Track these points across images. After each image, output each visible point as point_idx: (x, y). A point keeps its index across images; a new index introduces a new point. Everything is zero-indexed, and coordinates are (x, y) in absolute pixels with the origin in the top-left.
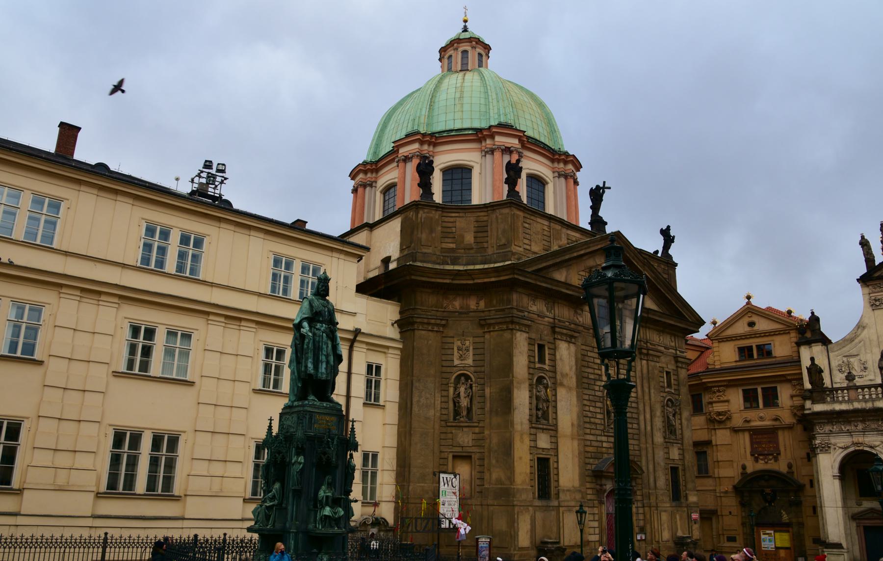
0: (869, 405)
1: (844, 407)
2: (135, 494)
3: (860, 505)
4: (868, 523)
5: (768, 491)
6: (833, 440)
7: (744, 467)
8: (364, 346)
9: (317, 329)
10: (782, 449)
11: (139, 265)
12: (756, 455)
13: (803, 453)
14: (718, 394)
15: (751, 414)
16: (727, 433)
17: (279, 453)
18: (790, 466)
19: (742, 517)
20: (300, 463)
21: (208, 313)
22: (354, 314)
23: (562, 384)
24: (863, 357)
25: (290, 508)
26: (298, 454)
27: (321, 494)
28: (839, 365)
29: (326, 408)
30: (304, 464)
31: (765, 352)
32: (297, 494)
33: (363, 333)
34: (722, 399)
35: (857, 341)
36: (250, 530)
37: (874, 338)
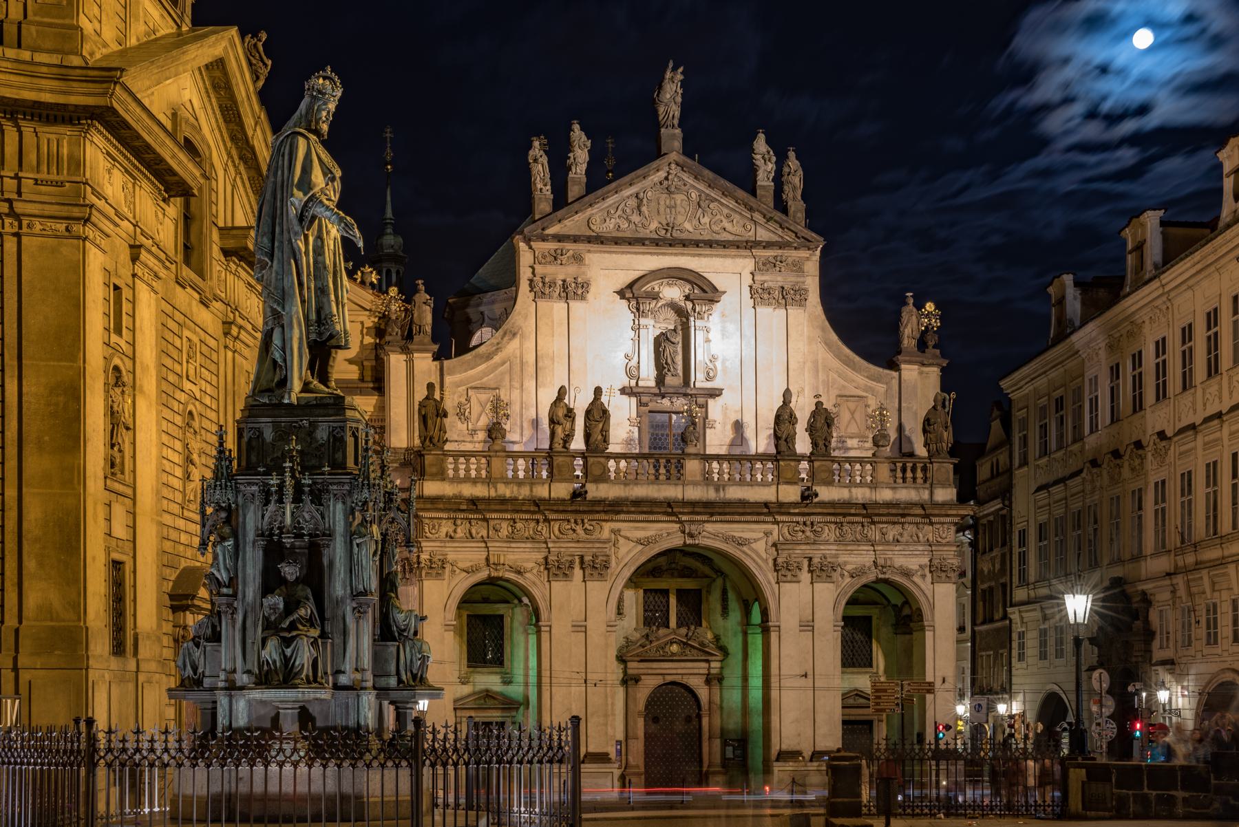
0: (524, 492)
1: (480, 491)
23: (142, 391)
24: (504, 395)
28: (460, 405)
35: (497, 359)
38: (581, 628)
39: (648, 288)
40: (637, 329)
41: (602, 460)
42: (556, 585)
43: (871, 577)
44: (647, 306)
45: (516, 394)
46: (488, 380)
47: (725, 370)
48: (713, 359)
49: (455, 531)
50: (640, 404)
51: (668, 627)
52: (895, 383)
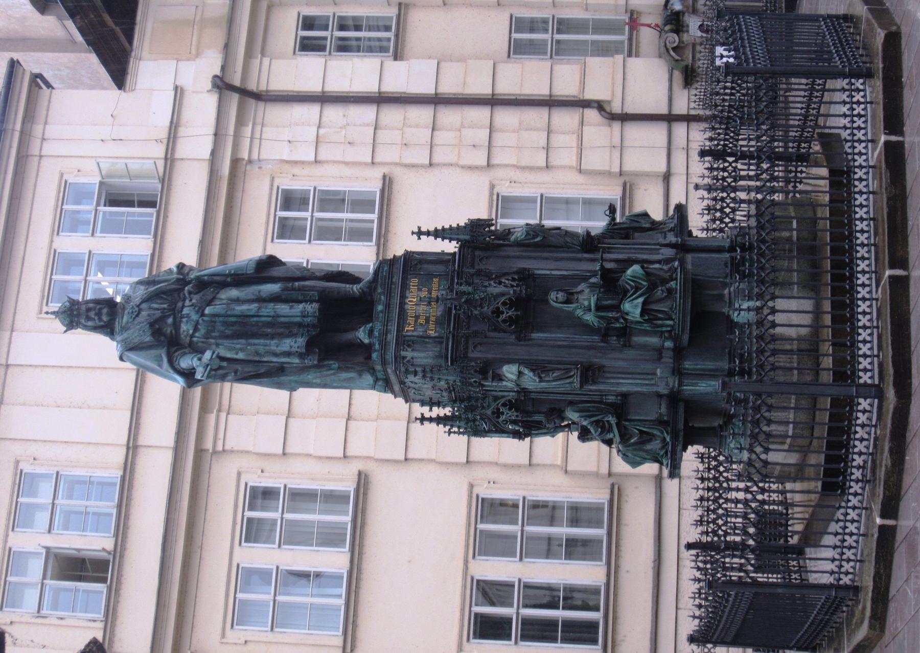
2: (608, 585)
8: (256, 62)
9: (196, 329)
11: (101, 616)
17: (498, 413)
20: (520, 373)
21: (200, 452)
22: (179, 92)
25: (627, 385)
26: (499, 378)
27: (589, 318)
29: (388, 306)
30: (521, 362)
32: (590, 373)
33: (223, 68)
36: (674, 472)
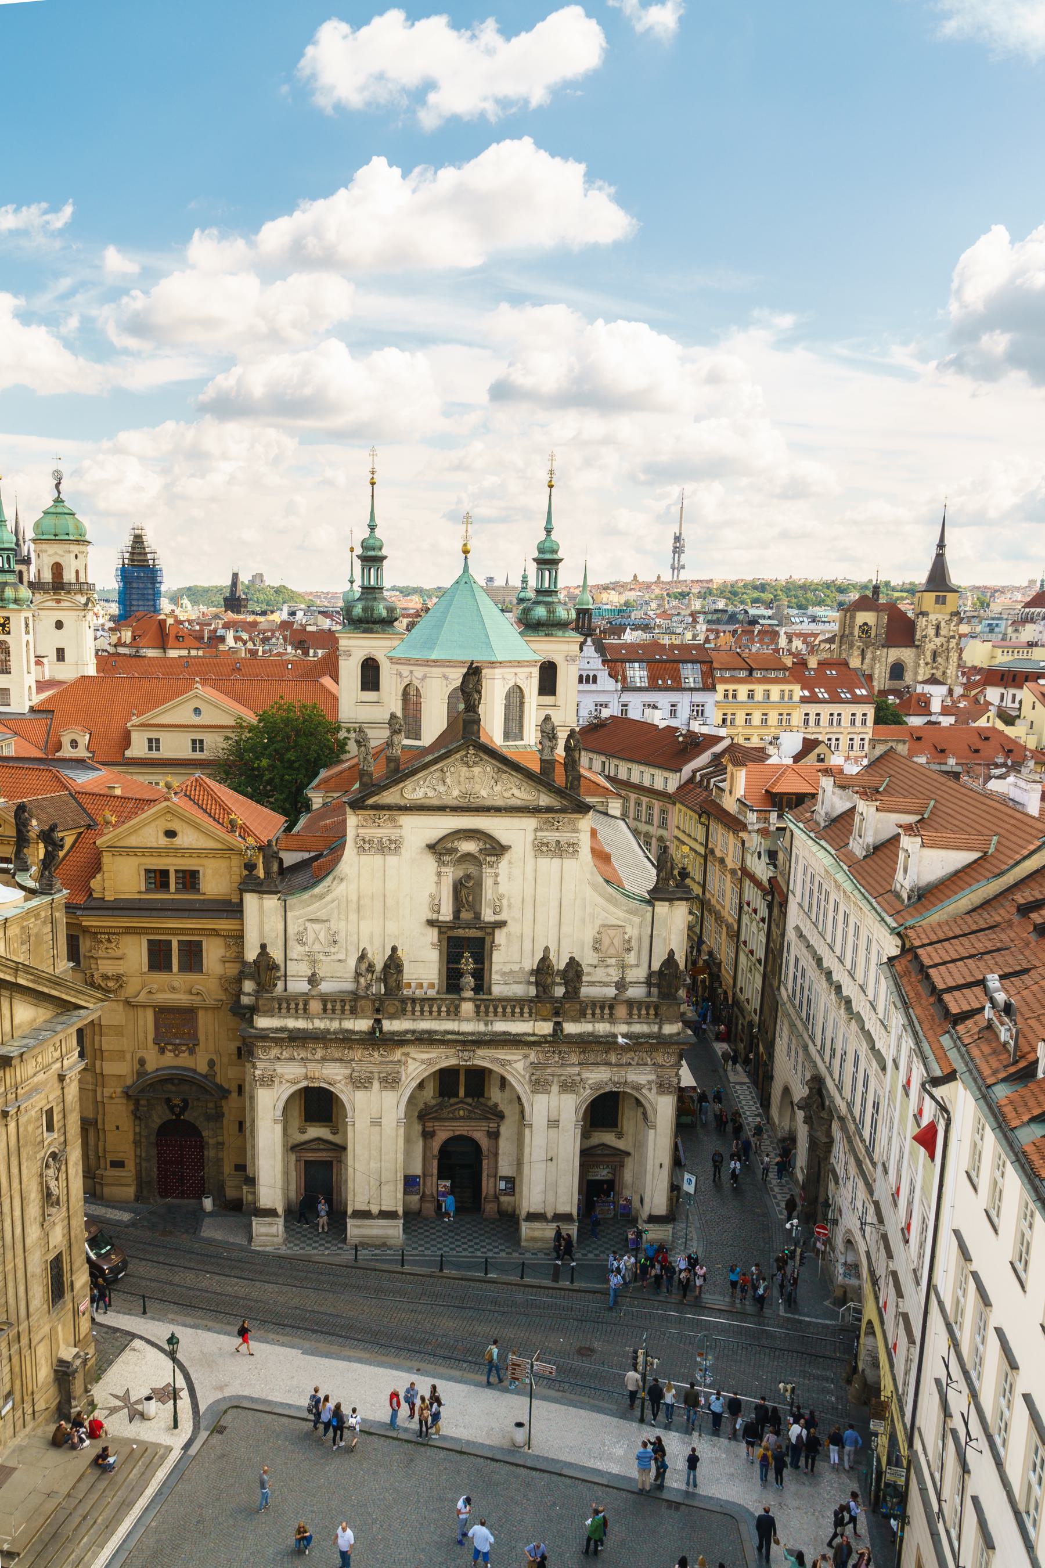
3: (303, 1131)
4: (311, 1156)
5: (177, 1101)
6: (279, 1071)
7: (142, 1062)
10: (202, 1037)
12: (161, 1043)
13: (233, 1047)
14: (107, 945)
15: (160, 978)
16: (120, 1007)
18: (211, 1064)
19: (135, 1134)
24: (333, 925)
28: (298, 933)
31: (190, 879)
34: (112, 953)
35: (328, 898)
37: (355, 899)
38: (376, 1122)
39: (450, 845)
40: (439, 874)
41: (396, 1003)
42: (360, 1096)
43: (607, 1089)
44: (446, 858)
45: (342, 924)
46: (322, 914)
47: (509, 906)
48: (500, 898)
49: (281, 1054)
50: (440, 933)
51: (457, 1095)
52: (649, 915)
